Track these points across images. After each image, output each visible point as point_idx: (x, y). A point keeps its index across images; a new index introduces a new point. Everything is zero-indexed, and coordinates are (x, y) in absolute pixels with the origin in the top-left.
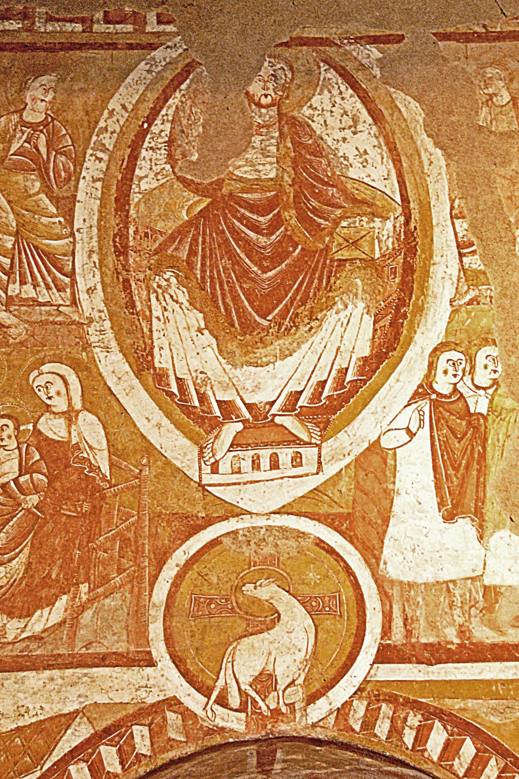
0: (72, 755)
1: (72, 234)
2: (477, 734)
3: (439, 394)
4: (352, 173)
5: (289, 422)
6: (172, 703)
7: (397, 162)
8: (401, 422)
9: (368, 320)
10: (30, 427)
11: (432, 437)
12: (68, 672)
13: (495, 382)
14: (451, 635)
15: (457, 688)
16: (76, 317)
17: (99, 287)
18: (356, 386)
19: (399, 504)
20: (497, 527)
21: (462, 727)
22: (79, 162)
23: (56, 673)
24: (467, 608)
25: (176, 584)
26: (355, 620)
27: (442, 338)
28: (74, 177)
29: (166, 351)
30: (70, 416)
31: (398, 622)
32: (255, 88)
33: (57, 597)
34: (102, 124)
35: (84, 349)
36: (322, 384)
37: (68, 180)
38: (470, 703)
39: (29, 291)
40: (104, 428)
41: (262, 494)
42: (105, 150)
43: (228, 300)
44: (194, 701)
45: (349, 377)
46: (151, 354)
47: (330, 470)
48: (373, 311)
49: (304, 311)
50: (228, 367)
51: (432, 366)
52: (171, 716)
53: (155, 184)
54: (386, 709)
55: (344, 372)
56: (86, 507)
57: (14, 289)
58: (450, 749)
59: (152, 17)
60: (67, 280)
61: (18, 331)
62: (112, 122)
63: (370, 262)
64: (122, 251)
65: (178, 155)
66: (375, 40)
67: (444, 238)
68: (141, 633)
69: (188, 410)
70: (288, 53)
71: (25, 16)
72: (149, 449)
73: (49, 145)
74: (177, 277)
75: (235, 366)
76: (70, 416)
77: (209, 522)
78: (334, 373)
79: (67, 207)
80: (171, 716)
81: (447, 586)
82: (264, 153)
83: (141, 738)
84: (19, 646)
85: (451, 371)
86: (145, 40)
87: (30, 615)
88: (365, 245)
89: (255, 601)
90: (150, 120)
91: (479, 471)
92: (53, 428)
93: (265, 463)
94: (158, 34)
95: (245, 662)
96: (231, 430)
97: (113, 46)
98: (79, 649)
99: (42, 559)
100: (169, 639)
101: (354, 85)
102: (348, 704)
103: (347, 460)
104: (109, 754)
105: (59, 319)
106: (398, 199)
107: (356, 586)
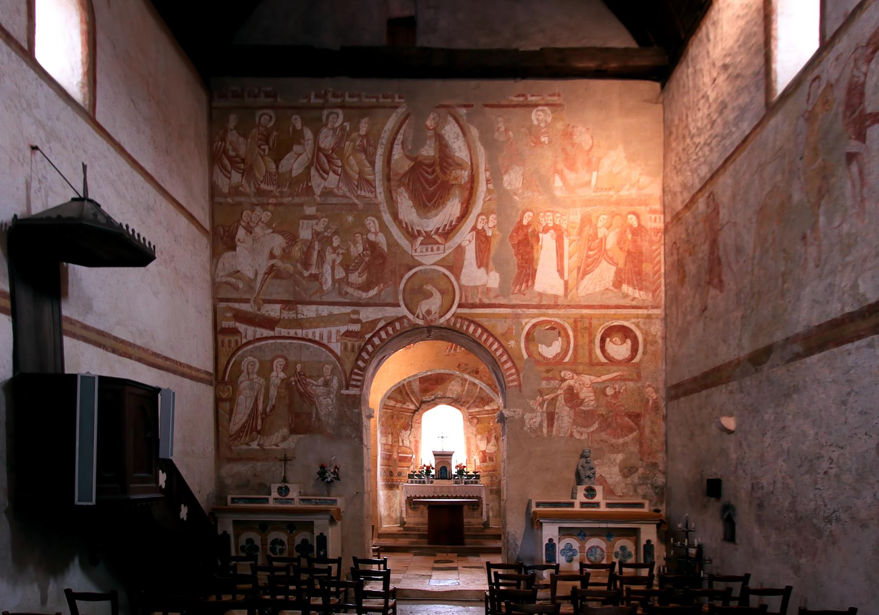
0: (381, 329)
4: (457, 154)
5: (436, 237)
6: (405, 317)
7: (470, 151)
8: (468, 238)
9: (459, 205)
14: (478, 301)
18: (456, 226)
19: (466, 263)
21: (478, 325)
22: (376, 149)
28: (374, 154)
30: (376, 233)
31: (464, 297)
32: (428, 123)
36: (446, 225)
39: (363, 193)
41: (429, 259)
42: (382, 144)
44: (411, 316)
47: (447, 252)
51: (477, 220)
52: (405, 320)
54: (459, 320)
55: (452, 222)
57: (359, 192)
58: (475, 331)
59: (397, 97)
61: (361, 206)
62: (385, 135)
63: (460, 185)
66: (465, 106)
67: (483, 176)
69: (408, 233)
71: (359, 96)
72: (398, 244)
76: (376, 233)
77: (414, 267)
79: (372, 164)
81: (476, 287)
82: (431, 147)
90: (397, 133)
92: (372, 237)
93: (430, 250)
94: (399, 103)
95: (424, 307)
97: (385, 107)
98: (381, 301)
100: (404, 300)
102: (449, 319)
104: (390, 329)
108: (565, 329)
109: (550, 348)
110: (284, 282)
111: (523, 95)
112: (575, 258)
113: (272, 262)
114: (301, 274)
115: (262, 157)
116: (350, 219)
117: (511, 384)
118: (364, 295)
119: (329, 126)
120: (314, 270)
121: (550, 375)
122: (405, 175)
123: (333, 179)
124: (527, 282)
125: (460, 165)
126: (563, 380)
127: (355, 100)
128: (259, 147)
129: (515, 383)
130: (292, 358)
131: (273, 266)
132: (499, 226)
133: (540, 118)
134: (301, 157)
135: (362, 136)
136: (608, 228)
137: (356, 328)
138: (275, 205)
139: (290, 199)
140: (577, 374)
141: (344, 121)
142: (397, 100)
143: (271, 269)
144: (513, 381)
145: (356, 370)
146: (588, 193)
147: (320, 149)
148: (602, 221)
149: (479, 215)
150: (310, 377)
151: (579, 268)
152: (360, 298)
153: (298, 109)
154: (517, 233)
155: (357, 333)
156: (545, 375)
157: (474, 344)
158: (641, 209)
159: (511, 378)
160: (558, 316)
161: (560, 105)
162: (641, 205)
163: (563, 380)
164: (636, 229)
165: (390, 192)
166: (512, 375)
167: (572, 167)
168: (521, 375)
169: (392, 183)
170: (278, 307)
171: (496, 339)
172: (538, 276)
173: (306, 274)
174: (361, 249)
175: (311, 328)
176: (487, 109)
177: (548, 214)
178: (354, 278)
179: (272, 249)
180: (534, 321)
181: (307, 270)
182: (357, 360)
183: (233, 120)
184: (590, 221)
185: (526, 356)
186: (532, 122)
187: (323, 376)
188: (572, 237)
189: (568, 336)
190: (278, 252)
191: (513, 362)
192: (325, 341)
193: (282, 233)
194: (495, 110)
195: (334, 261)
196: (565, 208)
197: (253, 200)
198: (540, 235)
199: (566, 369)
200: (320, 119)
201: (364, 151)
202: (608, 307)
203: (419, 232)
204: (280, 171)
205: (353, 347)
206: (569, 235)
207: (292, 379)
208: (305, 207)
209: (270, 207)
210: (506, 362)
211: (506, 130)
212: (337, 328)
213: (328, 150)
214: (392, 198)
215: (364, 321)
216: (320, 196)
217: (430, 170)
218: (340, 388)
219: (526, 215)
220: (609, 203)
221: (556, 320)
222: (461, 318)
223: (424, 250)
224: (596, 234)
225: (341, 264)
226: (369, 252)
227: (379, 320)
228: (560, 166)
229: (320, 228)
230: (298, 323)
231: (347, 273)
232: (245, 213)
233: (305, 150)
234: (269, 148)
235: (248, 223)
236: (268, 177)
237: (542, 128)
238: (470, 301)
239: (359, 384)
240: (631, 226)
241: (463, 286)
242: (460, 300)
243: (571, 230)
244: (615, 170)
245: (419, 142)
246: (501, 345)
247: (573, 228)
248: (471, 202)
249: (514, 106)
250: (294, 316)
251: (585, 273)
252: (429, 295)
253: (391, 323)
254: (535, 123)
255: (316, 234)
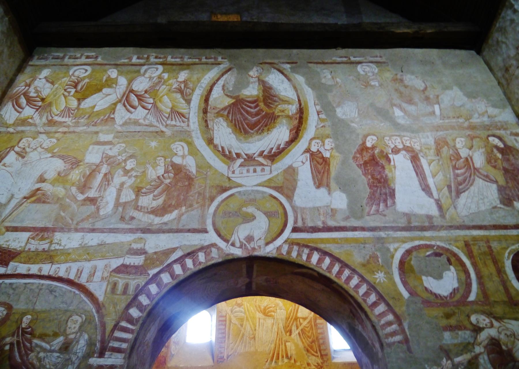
0: (175, 261)
1: (190, 108)
2: (331, 255)
3: (312, 152)
4: (282, 94)
6: (214, 245)
7: (296, 91)
10: (169, 160)
11: (311, 164)
12: (176, 234)
13: (332, 149)
14: (320, 224)
15: (322, 241)
16: (188, 130)
17: (197, 122)
18: (284, 149)
19: (299, 184)
20: (335, 191)
21: (325, 253)
22: (193, 90)
23: (171, 234)
24: (325, 215)
25: (218, 207)
26: (284, 219)
27: (313, 136)
28: (191, 94)
29: (218, 139)
30: (183, 157)
32: (251, 73)
33: (173, 211)
34: (202, 81)
35: (190, 138)
36: (272, 149)
37: (190, 94)
38: (328, 245)
39: (173, 123)
40: (195, 160)
42: (202, 87)
43: (240, 125)
44: (222, 244)
45: (281, 147)
46: (213, 139)
47: (274, 173)
48: (290, 129)
49: (266, 129)
50: (239, 144)
52: (214, 250)
53: (218, 96)
56: (187, 183)
57: (169, 122)
60: (186, 120)
61: (168, 132)
63: (288, 116)
64: (205, 112)
65: (225, 88)
66: (288, 63)
68: (204, 223)
69: (224, 155)
70: (261, 65)
71: (181, 58)
72: (210, 167)
73: (185, 86)
74: (223, 119)
75: (242, 143)
78: (276, 145)
79: (188, 102)
80: (214, 250)
81: (318, 209)
82: (253, 88)
83: (201, 257)
84: (158, 226)
85: (316, 145)
86: (217, 62)
87: (163, 216)
88: (286, 112)
89: (247, 213)
90: (218, 80)
91: (328, 174)
92: (177, 160)
95: (242, 232)
96: (240, 161)
98: (180, 227)
99: (169, 199)
100: (214, 224)
101: (282, 73)
103: (281, 170)
105: (183, 130)
106: (297, 100)
107: (284, 208)
108: (455, 255)
109: (441, 282)
110: (46, 207)
111: (346, 57)
112: (440, 176)
113: (38, 186)
114: (74, 198)
115: (65, 97)
116: (153, 144)
117: (391, 340)
118: (157, 220)
119: (147, 75)
120: (92, 194)
121: (453, 321)
122: (225, 109)
123: (140, 113)
124: (385, 201)
125: (287, 102)
126: (477, 330)
127: (178, 60)
128: (65, 90)
129: (398, 338)
130: (20, 306)
131: (38, 189)
132: (337, 148)
133: (366, 70)
134: (110, 96)
135: (181, 82)
136: (470, 149)
137: (138, 260)
138: (65, 133)
139: (85, 127)
140: (498, 319)
141: (163, 72)
142: (220, 59)
143: (34, 193)
144: (393, 334)
145: (124, 324)
146: (437, 121)
147: (132, 91)
148: (460, 143)
149: (312, 140)
150: (42, 337)
151: (449, 187)
152: (151, 224)
153: (116, 65)
154: (361, 154)
155: (136, 267)
156: (444, 322)
157: (318, 286)
158: (502, 132)
159: (389, 329)
160: (441, 239)
161: (384, 63)
162: (500, 129)
163: (477, 330)
164: (502, 149)
165: (206, 121)
166: (390, 324)
167: (410, 102)
168: (406, 325)
169: (209, 115)
170: (26, 235)
171: (354, 271)
172: (398, 195)
173: (81, 197)
174: (161, 171)
175: (66, 262)
176: (310, 65)
177: (395, 138)
178: (146, 201)
179: (45, 172)
180: (408, 246)
181: (82, 193)
182: (129, 306)
183: (46, 72)
184: (447, 143)
185: (406, 294)
186: (358, 73)
187: (64, 334)
188: (429, 158)
189: (463, 264)
190: (51, 175)
191: (388, 304)
192: (83, 281)
193: (62, 157)
194: (319, 65)
195: (122, 184)
196: (413, 132)
197: (42, 130)
198: (391, 156)
199: (476, 312)
200: (139, 71)
201: (181, 91)
202: (505, 227)
203: (238, 155)
204: (82, 107)
205: (126, 287)
206: (425, 156)
207: (8, 340)
208: (100, 135)
209: (57, 135)
210: (375, 304)
211: (333, 78)
212: (105, 262)
213: (141, 92)
214: (207, 126)
215: (151, 251)
216: (120, 126)
217: (252, 105)
218: (89, 355)
219: (369, 138)
220: (461, 127)
221: (438, 243)
222: (298, 244)
223: (245, 171)
224: (458, 154)
225: (131, 187)
226: (171, 175)
227: (173, 250)
228: (397, 101)
229: (113, 152)
230: (49, 257)
231: (137, 196)
232: (24, 140)
233: (116, 92)
234: (76, 91)
235: (24, 149)
236: (68, 111)
237: (369, 76)
238: (310, 224)
239: (124, 346)
240: (497, 147)
241: (297, 207)
242: (296, 222)
243: (427, 151)
244: (458, 103)
245: (241, 84)
246: (363, 280)
247: (429, 149)
248: (302, 128)
249: (339, 63)
250: (46, 247)
251: (459, 193)
252: (249, 218)
253: (192, 254)
254: (362, 73)
255: (107, 159)
